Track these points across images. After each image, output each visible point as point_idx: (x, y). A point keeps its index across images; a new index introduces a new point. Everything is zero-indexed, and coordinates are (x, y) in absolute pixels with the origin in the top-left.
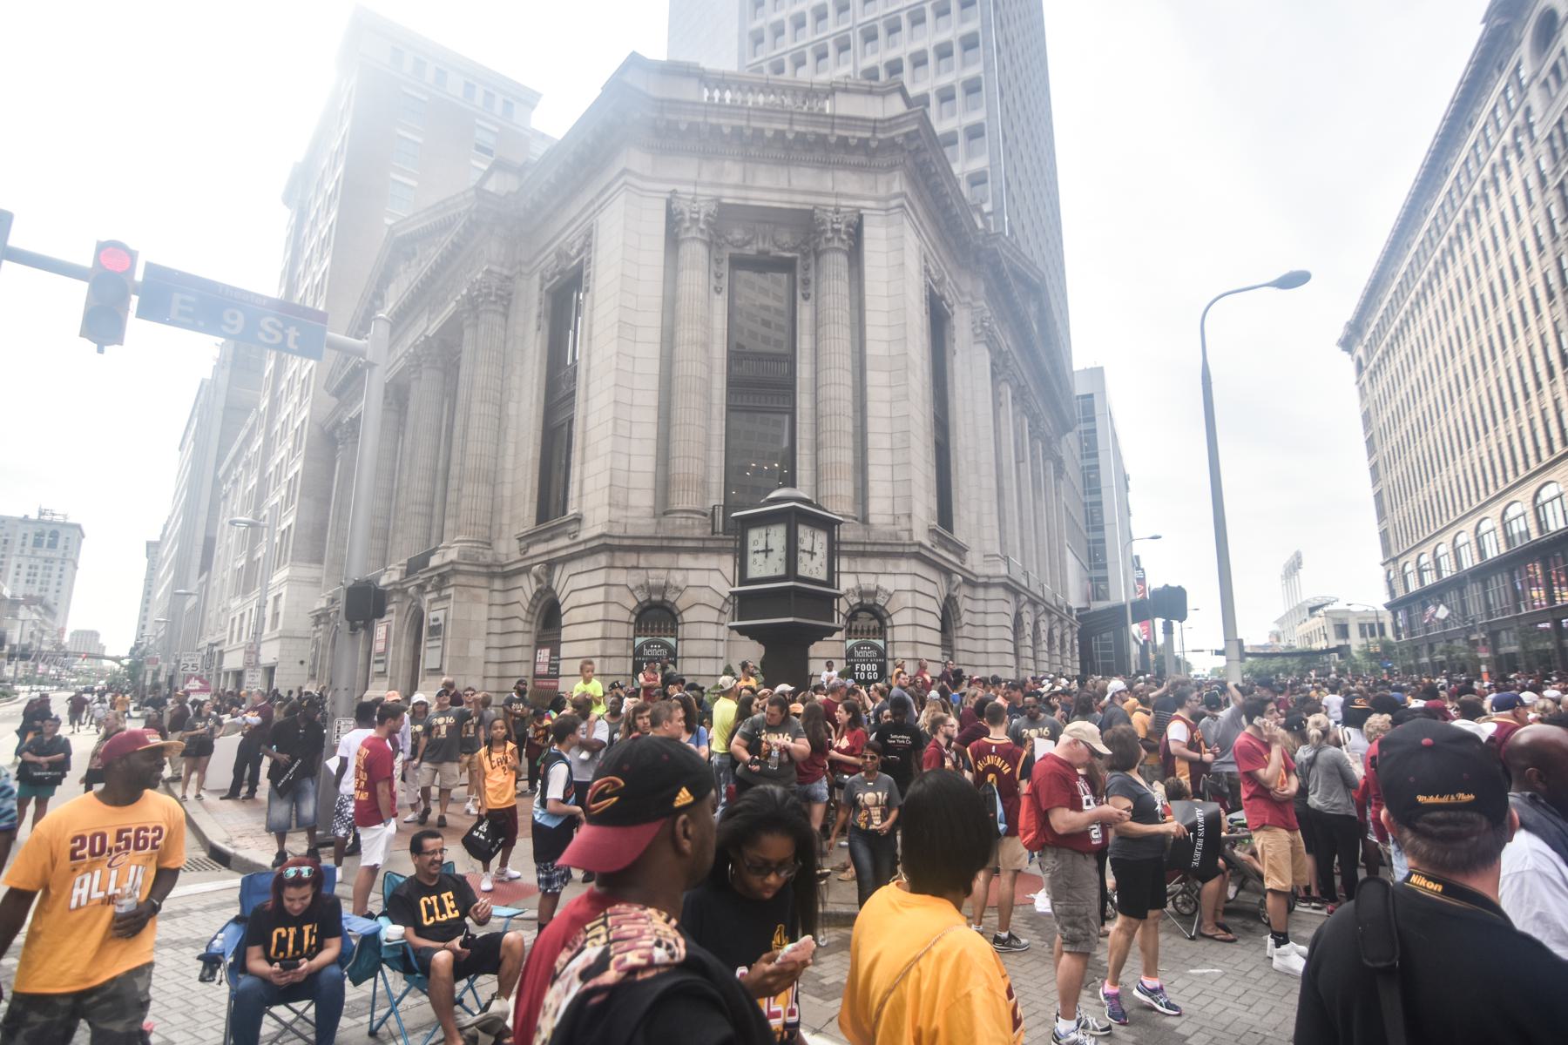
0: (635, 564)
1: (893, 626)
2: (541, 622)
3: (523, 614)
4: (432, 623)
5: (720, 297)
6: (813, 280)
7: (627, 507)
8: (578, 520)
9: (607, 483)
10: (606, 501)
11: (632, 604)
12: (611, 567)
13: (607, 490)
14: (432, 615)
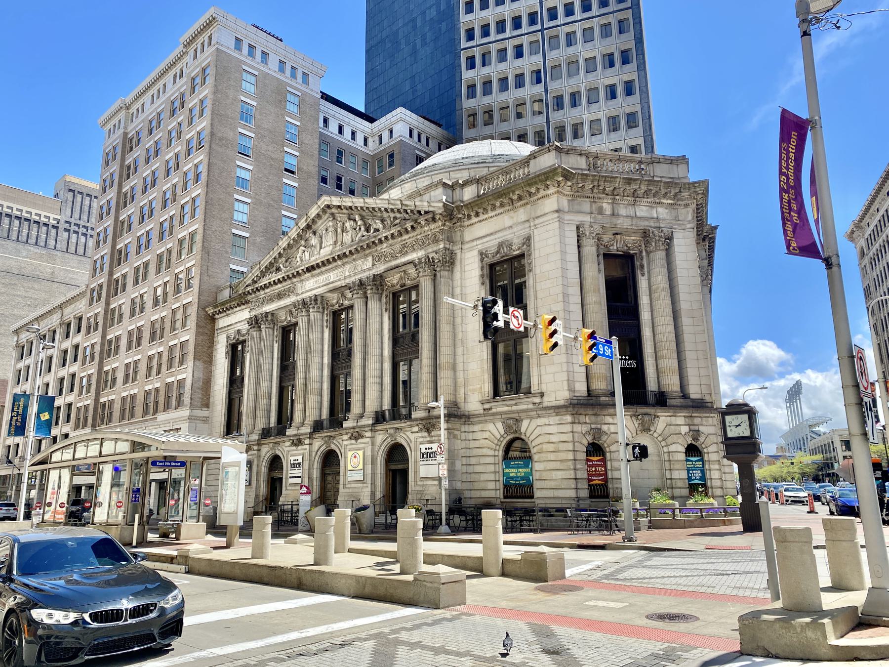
6: (645, 265)
7: (574, 391)
8: (542, 395)
9: (566, 378)
10: (566, 388)
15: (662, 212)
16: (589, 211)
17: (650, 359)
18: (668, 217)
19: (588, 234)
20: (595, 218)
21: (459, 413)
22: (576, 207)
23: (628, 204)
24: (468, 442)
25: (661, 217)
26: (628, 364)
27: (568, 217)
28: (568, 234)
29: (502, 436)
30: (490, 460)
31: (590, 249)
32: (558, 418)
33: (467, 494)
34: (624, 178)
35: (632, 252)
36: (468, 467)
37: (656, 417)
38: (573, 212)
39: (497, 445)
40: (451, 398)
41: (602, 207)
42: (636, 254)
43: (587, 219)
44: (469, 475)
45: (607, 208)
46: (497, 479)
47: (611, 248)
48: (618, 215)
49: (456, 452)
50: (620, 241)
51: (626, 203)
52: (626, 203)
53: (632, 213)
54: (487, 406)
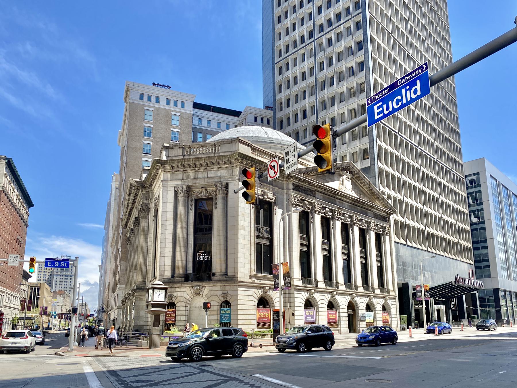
1: (218, 306)
5: (192, 212)
7: (164, 276)
15: (223, 173)
16: (182, 178)
18: (226, 175)
19: (180, 191)
20: (184, 182)
22: (175, 177)
23: (204, 171)
25: (222, 175)
26: (206, 258)
27: (170, 183)
28: (169, 192)
31: (181, 198)
34: (194, 158)
35: (210, 196)
37: (205, 287)
38: (172, 180)
40: (142, 280)
41: (189, 175)
42: (213, 197)
43: (180, 182)
45: (192, 175)
47: (199, 196)
48: (198, 178)
50: (203, 192)
51: (202, 170)
52: (202, 170)
53: (206, 176)
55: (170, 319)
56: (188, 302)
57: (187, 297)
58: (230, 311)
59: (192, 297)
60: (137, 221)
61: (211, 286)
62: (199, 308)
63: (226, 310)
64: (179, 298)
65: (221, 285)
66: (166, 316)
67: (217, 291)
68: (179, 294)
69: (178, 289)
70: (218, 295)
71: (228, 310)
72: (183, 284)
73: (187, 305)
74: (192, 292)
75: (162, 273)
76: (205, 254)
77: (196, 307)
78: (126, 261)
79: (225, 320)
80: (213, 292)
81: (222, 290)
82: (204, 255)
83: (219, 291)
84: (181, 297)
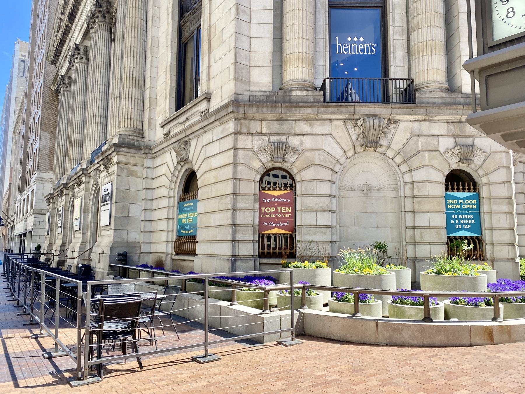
0: (259, 131)
2: (181, 189)
3: (167, 183)
4: (104, 193)
7: (248, 83)
8: (208, 98)
9: (233, 60)
10: (232, 76)
11: (257, 165)
12: (237, 133)
13: (232, 67)
14: (104, 188)
17: (397, 37)
21: (142, 144)
24: (150, 181)
26: (362, 50)
29: (176, 168)
30: (164, 203)
32: (220, 128)
33: (144, 248)
36: (148, 213)
39: (171, 181)
40: (136, 124)
44: (148, 224)
46: (170, 228)
49: (132, 193)
54: (166, 130)
55: (276, 220)
56: (337, 168)
57: (338, 153)
58: (475, 201)
59: (351, 153)
60: (100, 9)
61: (415, 121)
62: (362, 190)
63: (464, 199)
64: (307, 154)
65: (451, 118)
66: (260, 210)
67: (438, 136)
68: (309, 142)
69: (303, 127)
70: (442, 150)
71: (468, 198)
72: (322, 110)
73: (335, 178)
74: (354, 137)
75: (244, 75)
76: (358, 38)
77: (352, 189)
78: (53, 133)
79: (462, 229)
80: (423, 140)
81: (455, 136)
82: (355, 39)
83: (442, 136)
84: (316, 150)
